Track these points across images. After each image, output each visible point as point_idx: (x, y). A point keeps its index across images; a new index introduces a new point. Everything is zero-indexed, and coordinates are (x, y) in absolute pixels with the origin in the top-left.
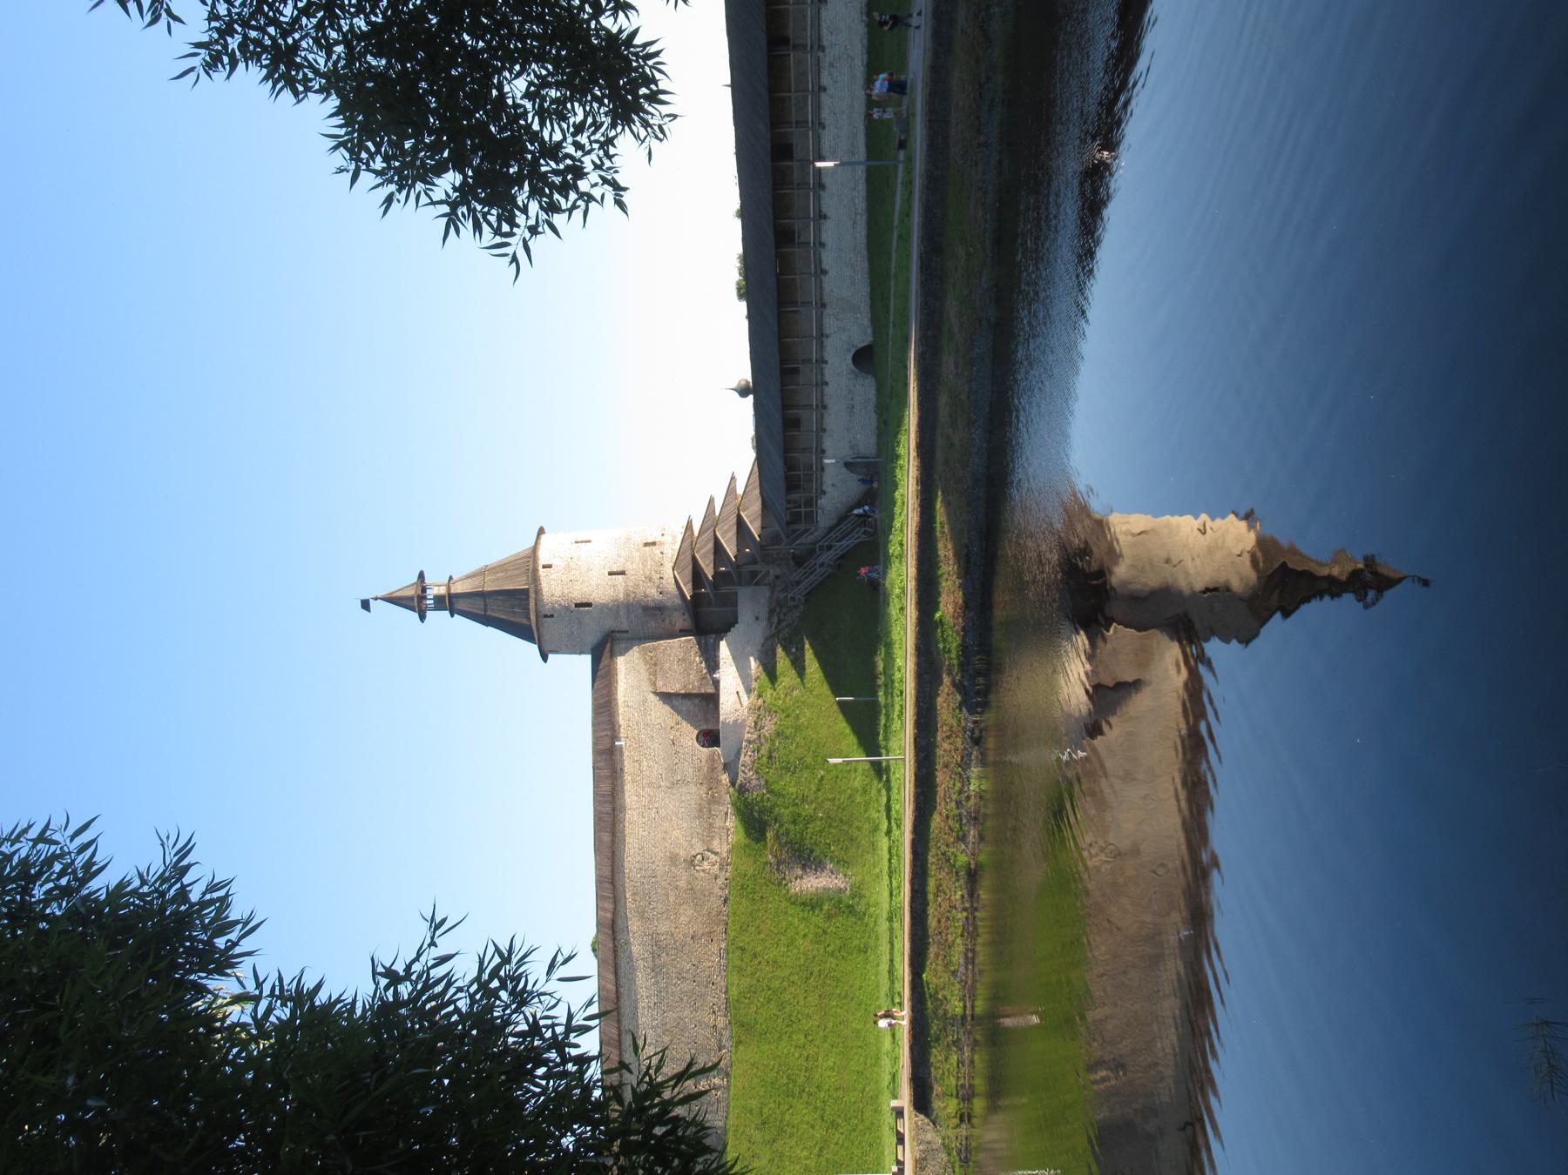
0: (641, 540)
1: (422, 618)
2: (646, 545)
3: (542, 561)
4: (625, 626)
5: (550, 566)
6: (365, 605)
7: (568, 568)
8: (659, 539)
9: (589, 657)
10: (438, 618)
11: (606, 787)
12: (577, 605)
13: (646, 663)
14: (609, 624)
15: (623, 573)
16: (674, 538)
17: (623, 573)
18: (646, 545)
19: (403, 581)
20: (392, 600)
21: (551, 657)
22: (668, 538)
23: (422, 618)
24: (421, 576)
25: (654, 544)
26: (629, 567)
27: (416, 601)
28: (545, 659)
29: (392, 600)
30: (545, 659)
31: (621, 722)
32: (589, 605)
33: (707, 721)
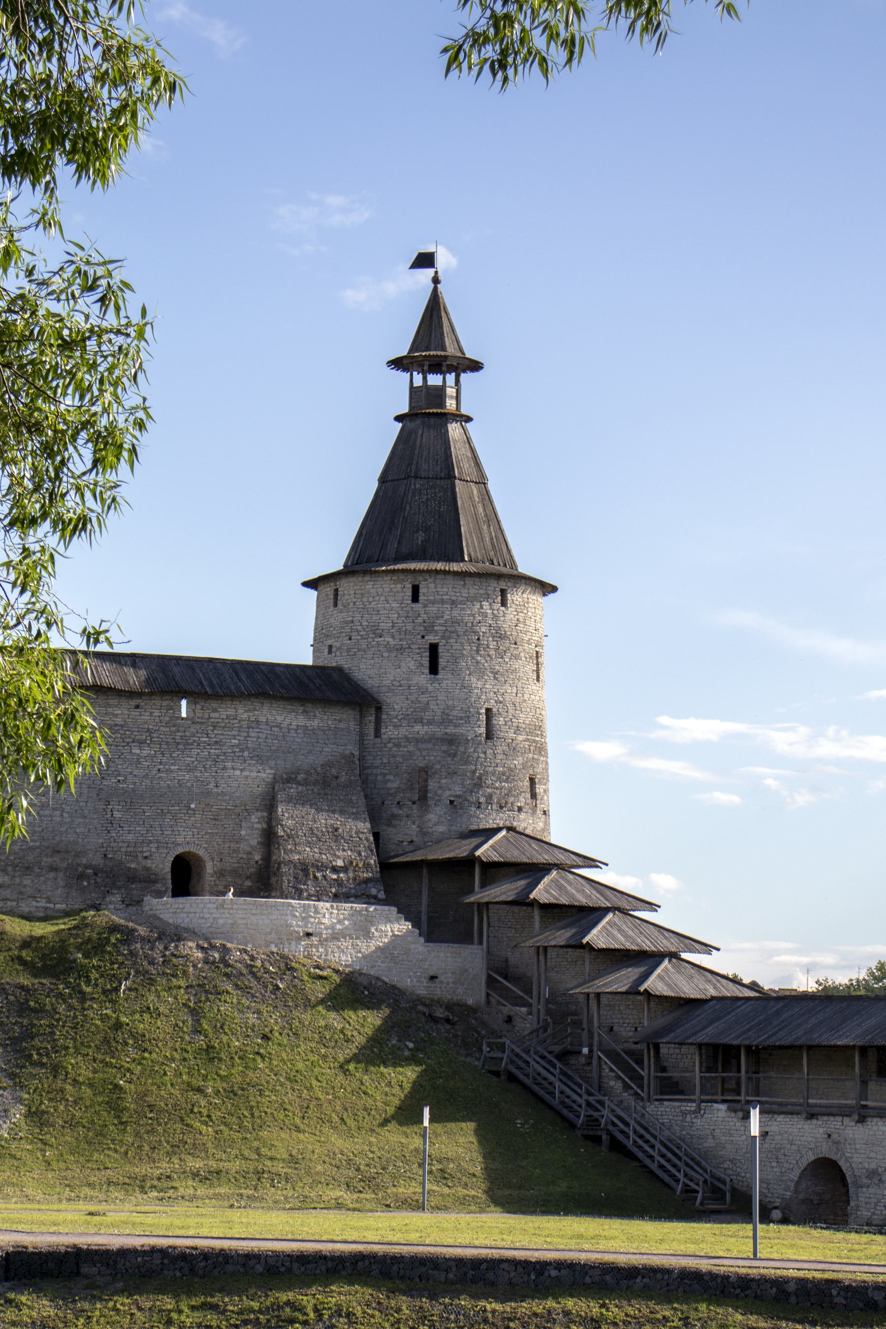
1: (397, 364)
2: (532, 781)
4: (389, 732)
6: (425, 260)
7: (500, 636)
10: (397, 392)
12: (434, 649)
13: (328, 765)
14: (396, 704)
15: (489, 735)
17: (489, 735)
18: (532, 781)
19: (468, 334)
20: (434, 312)
21: (313, 594)
23: (397, 364)
24: (475, 366)
25: (534, 796)
26: (501, 748)
27: (433, 350)
28: (310, 584)
29: (434, 312)
30: (310, 584)
33: (220, 874)
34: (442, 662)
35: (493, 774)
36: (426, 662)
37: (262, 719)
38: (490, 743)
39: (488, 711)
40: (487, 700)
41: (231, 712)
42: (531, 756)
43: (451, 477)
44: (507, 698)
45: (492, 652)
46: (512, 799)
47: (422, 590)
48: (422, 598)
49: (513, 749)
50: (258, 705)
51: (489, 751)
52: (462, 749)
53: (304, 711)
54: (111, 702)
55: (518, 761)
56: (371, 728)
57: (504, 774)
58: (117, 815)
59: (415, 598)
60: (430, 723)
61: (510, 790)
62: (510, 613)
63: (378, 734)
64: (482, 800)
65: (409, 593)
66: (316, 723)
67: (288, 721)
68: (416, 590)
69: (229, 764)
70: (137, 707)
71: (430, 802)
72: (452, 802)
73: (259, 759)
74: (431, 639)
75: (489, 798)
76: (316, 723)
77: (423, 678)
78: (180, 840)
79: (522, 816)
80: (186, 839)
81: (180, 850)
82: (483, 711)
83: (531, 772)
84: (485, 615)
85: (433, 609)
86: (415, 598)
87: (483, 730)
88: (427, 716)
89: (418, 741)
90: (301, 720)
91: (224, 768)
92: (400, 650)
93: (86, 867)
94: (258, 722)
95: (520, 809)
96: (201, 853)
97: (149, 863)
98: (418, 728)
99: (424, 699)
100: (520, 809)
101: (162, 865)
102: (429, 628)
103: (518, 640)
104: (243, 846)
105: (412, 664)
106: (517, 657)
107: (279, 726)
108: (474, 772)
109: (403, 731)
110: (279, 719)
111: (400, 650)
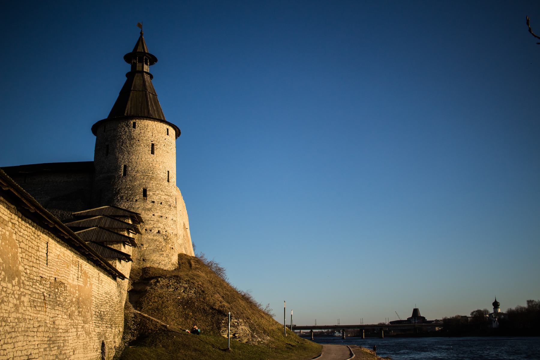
5: (134, 126)
8: (149, 199)
15: (125, 174)
18: (145, 191)
42: (144, 181)
44: (133, 160)
45: (128, 145)
46: (132, 197)
49: (134, 179)
62: (137, 130)
75: (122, 198)
79: (138, 203)
82: (123, 166)
84: (126, 132)
86: (104, 132)
87: (122, 173)
95: (136, 200)
100: (136, 200)
103: (140, 139)
106: (139, 146)
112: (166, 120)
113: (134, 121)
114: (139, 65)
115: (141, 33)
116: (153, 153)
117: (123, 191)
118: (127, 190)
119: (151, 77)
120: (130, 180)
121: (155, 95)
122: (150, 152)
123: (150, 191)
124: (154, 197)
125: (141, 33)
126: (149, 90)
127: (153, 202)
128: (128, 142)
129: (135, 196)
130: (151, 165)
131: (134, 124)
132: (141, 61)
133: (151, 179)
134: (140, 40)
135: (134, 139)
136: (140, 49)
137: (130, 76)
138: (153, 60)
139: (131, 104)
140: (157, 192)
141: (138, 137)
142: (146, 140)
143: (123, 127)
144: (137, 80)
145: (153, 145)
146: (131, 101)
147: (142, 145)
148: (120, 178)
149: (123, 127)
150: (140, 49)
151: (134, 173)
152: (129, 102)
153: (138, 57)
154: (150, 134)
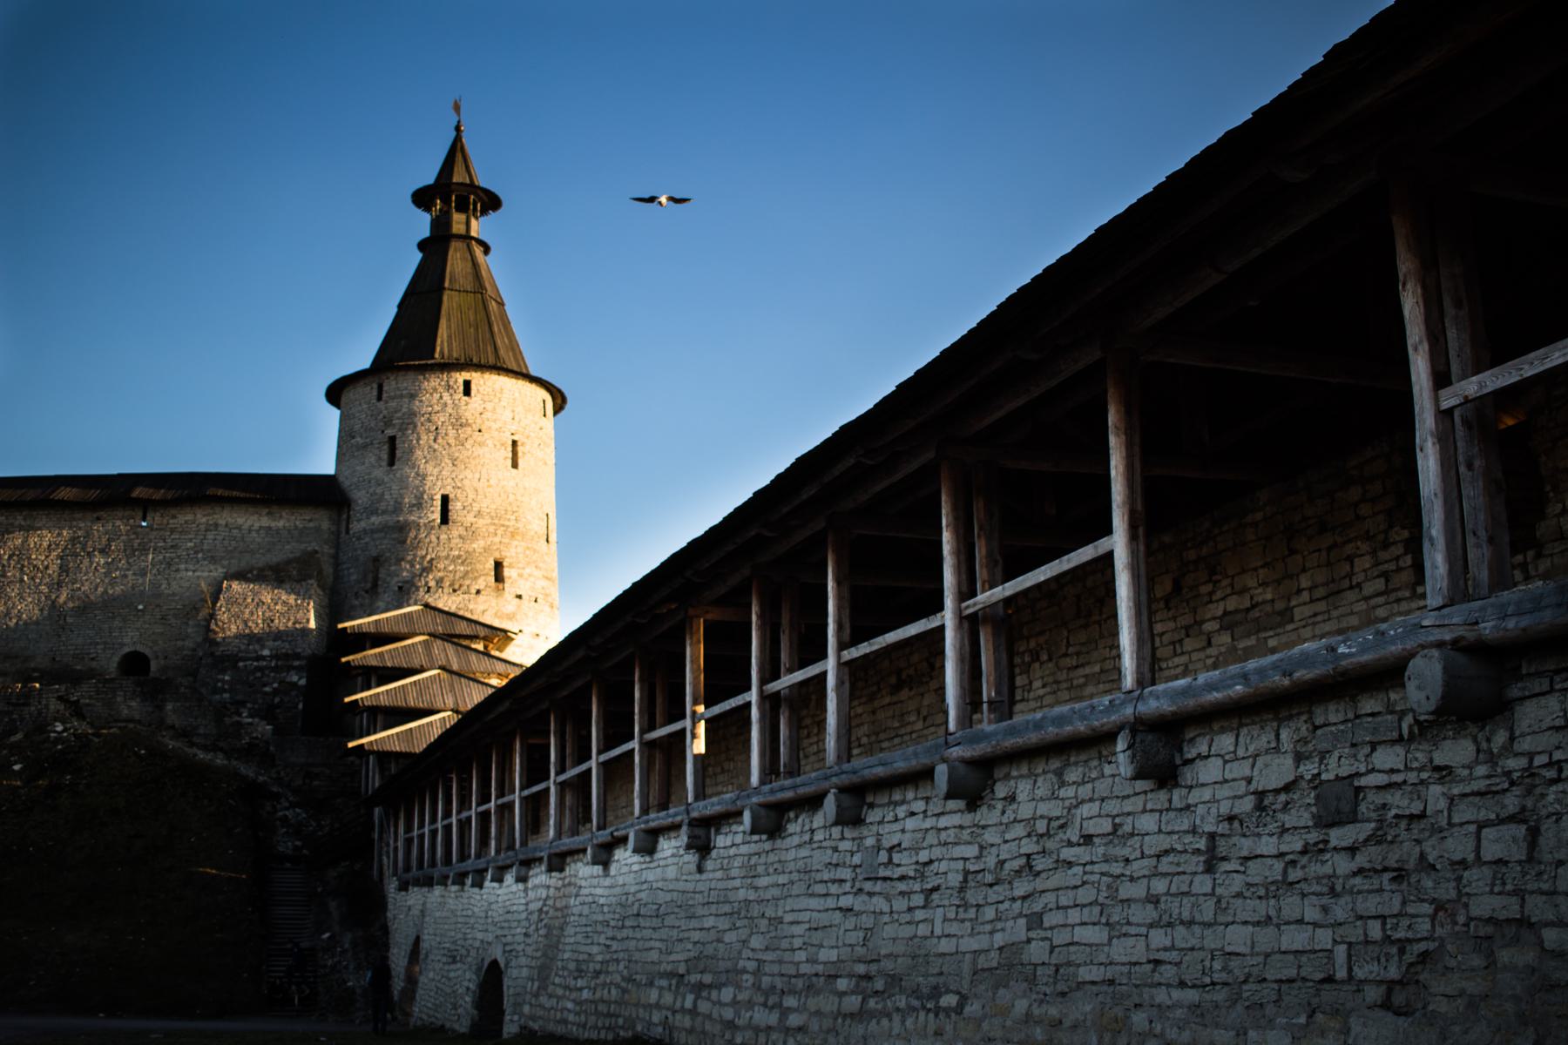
0: (512, 555)
2: (498, 566)
3: (476, 377)
4: (356, 527)
5: (467, 390)
7: (459, 423)
8: (510, 588)
9: (327, 466)
10: (422, 224)
11: (65, 493)
12: (392, 440)
14: (360, 497)
15: (445, 519)
16: (511, 617)
17: (445, 519)
18: (498, 566)
22: (510, 604)
25: (499, 577)
26: (455, 531)
31: (182, 519)
32: (392, 461)
34: (398, 453)
35: (447, 557)
36: (385, 456)
37: (222, 522)
38: (444, 527)
39: (445, 500)
40: (443, 486)
41: (189, 517)
42: (497, 540)
43: (441, 289)
44: (466, 482)
45: (452, 441)
46: (467, 582)
47: (385, 388)
48: (385, 396)
49: (471, 533)
50: (218, 509)
51: (444, 537)
52: (412, 534)
53: (269, 514)
54: (77, 516)
55: (478, 545)
56: (344, 524)
57: (459, 557)
58: (70, 620)
59: (379, 398)
60: (384, 512)
61: (467, 573)
62: (475, 401)
63: (347, 532)
64: (432, 584)
65: (375, 393)
66: (281, 524)
67: (250, 522)
68: (380, 388)
69: (182, 566)
70: (98, 519)
71: (380, 590)
72: (400, 588)
73: (213, 560)
74: (390, 432)
75: (439, 582)
76: (281, 524)
77: (379, 473)
78: (127, 640)
79: (481, 598)
80: (130, 640)
81: (127, 650)
82: (438, 497)
83: (497, 555)
84: (446, 405)
85: (393, 404)
86: (379, 398)
87: (437, 516)
88: (383, 506)
89: (373, 531)
90: (265, 521)
91: (177, 570)
92: (365, 446)
93: (34, 670)
94: (216, 525)
95: (478, 592)
96: (147, 652)
97: (94, 664)
98: (373, 519)
99: (379, 491)
101: (111, 664)
102: (388, 423)
104: (189, 644)
105: (373, 459)
107: (239, 528)
108: (423, 557)
109: (363, 524)
110: (240, 521)
111: (365, 446)
112: (533, 372)
113: (466, 375)
114: (458, 219)
115: (458, 129)
116: (515, 465)
117: (441, 566)
118: (453, 561)
119: (487, 249)
120: (460, 537)
121: (501, 304)
122: (509, 462)
123: (511, 566)
124: (521, 582)
125: (458, 129)
126: (490, 291)
127: (519, 597)
128: (452, 433)
129: (476, 578)
130: (512, 497)
131: (467, 384)
132: (462, 207)
133: (513, 535)
134: (456, 151)
135: (467, 425)
136: (459, 177)
137: (435, 247)
138: (491, 202)
139: (449, 327)
140: (528, 570)
141: (479, 421)
142: (499, 430)
143: (435, 390)
144: (456, 261)
145: (514, 443)
146: (449, 320)
147: (489, 442)
148: (432, 528)
149: (435, 390)
150: (459, 177)
151: (470, 518)
152: (443, 323)
153: (453, 196)
154: (508, 415)
